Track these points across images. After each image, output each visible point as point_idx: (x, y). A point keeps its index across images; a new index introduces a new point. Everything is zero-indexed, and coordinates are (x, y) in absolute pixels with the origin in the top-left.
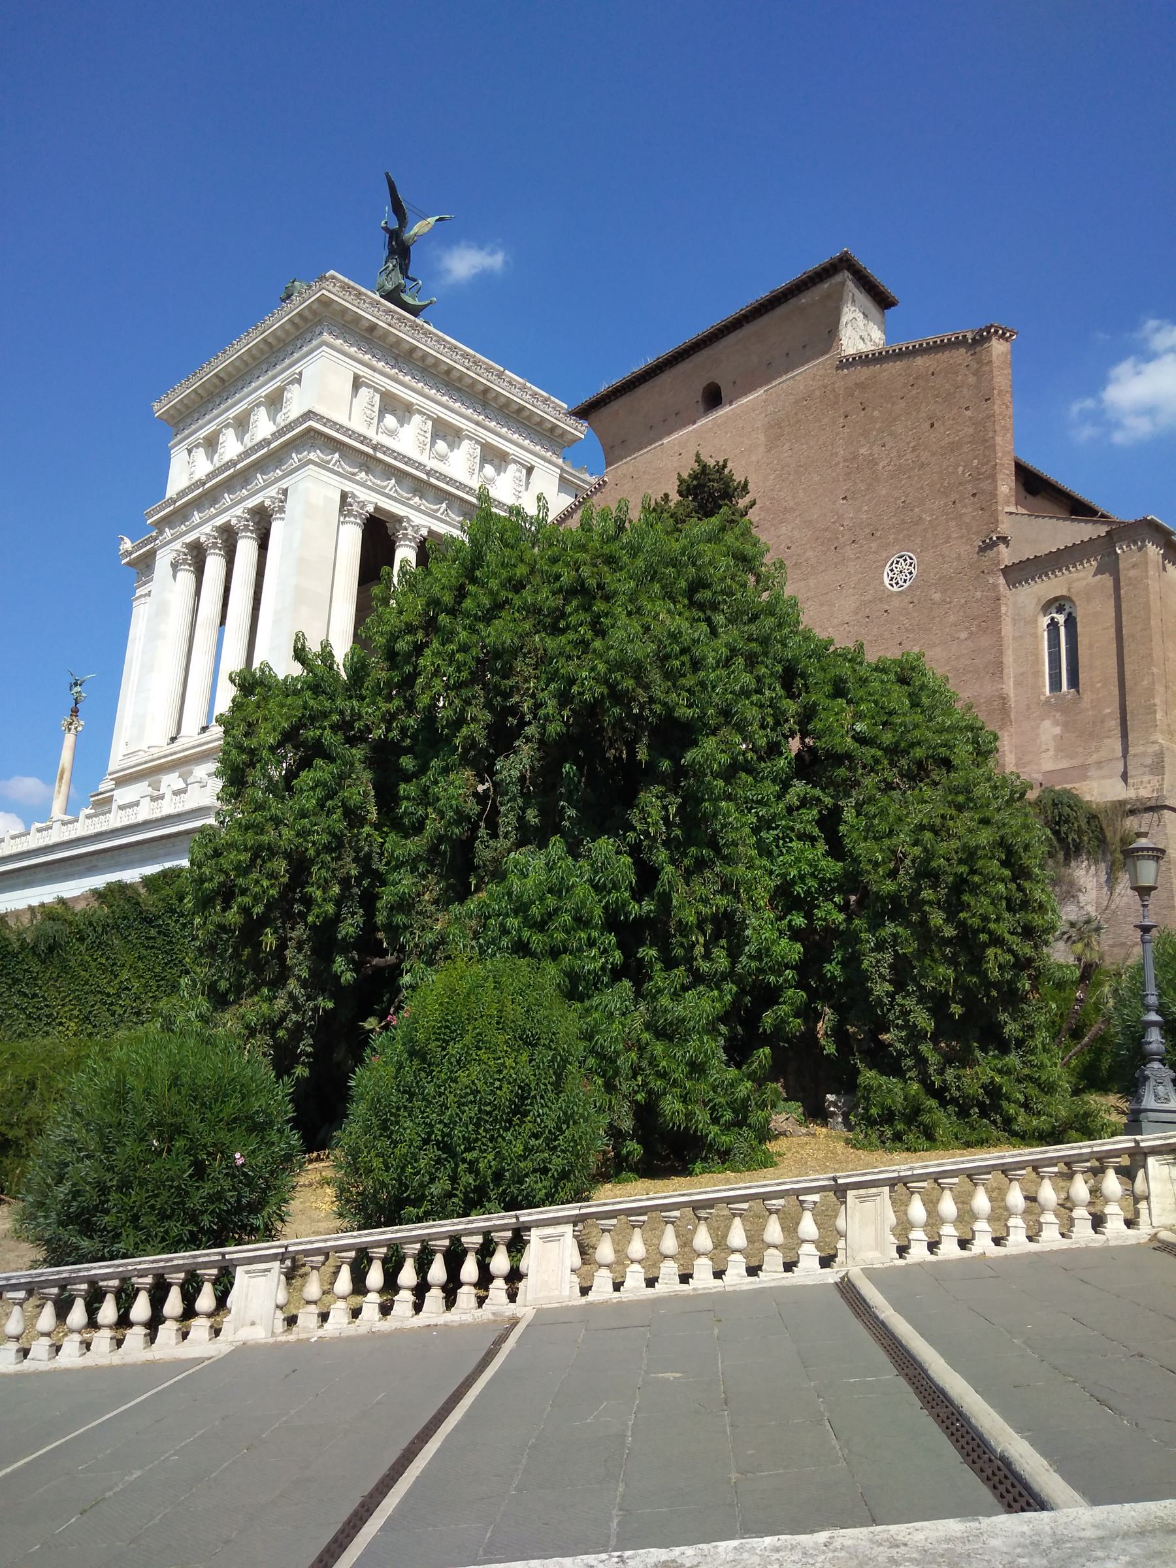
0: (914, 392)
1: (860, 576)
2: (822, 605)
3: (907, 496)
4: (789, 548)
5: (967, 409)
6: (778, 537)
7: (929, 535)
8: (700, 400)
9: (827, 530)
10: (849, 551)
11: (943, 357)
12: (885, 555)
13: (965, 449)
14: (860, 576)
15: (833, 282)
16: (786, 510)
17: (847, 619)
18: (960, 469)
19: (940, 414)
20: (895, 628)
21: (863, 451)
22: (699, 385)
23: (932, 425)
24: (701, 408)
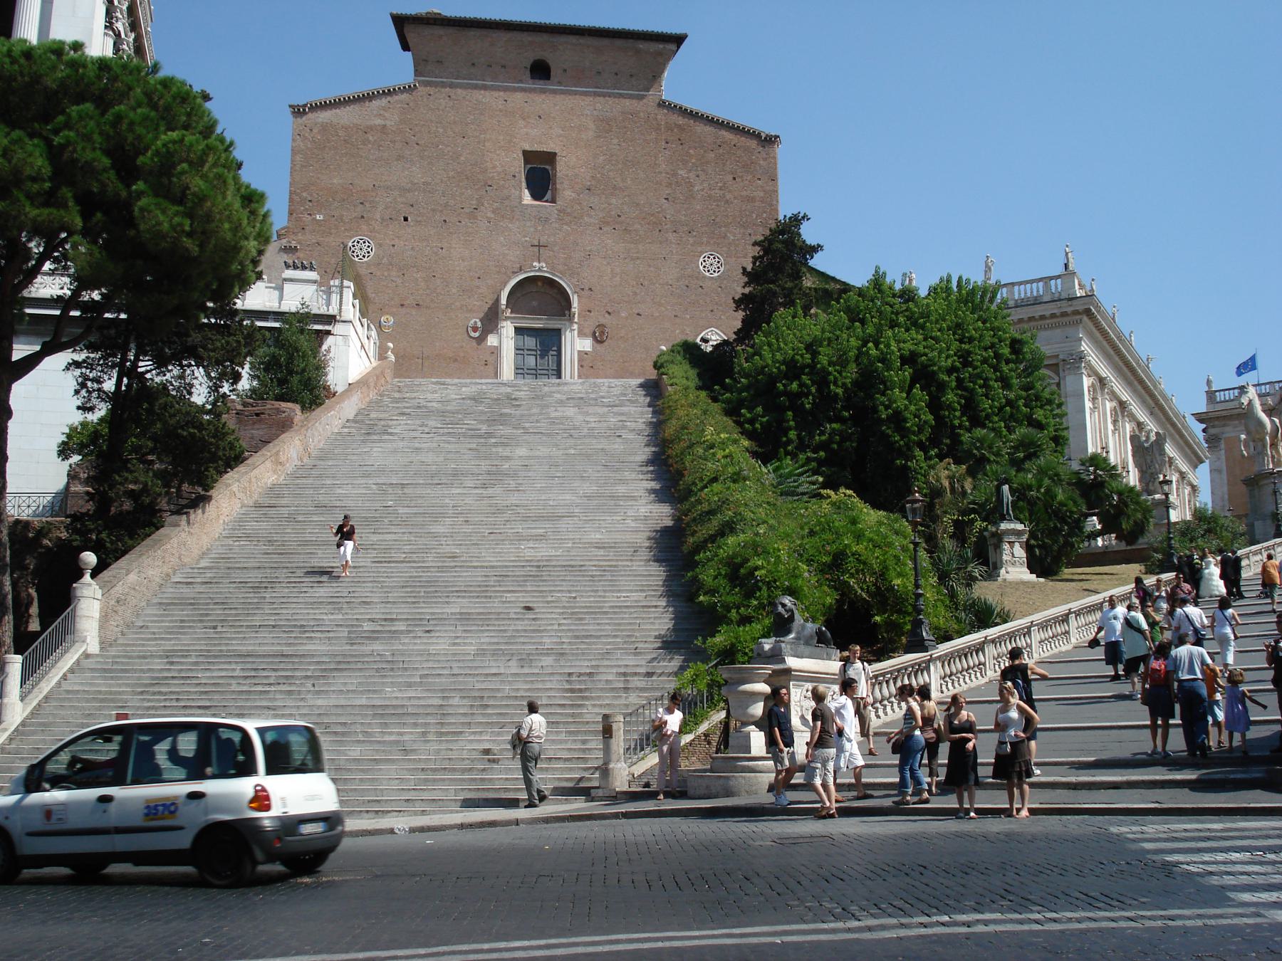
0: (721, 151)
1: (680, 257)
2: (650, 266)
3: (716, 217)
4: (619, 216)
5: (759, 179)
6: (610, 204)
7: (732, 248)
8: (529, 67)
9: (653, 215)
10: (671, 236)
11: (743, 140)
12: (699, 249)
13: (757, 204)
14: (680, 257)
15: (666, 46)
16: (615, 188)
17: (670, 282)
18: (754, 216)
19: (740, 174)
20: (708, 300)
21: (680, 172)
22: (530, 56)
23: (734, 179)
24: (528, 72)
